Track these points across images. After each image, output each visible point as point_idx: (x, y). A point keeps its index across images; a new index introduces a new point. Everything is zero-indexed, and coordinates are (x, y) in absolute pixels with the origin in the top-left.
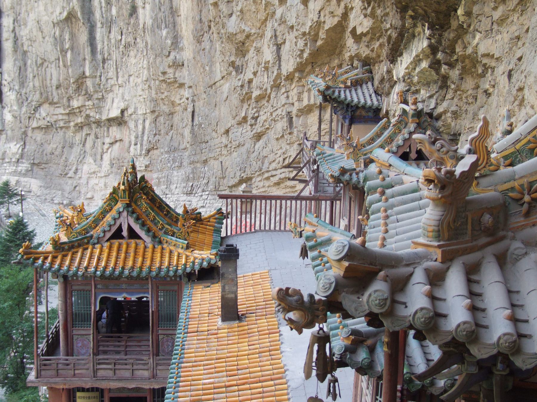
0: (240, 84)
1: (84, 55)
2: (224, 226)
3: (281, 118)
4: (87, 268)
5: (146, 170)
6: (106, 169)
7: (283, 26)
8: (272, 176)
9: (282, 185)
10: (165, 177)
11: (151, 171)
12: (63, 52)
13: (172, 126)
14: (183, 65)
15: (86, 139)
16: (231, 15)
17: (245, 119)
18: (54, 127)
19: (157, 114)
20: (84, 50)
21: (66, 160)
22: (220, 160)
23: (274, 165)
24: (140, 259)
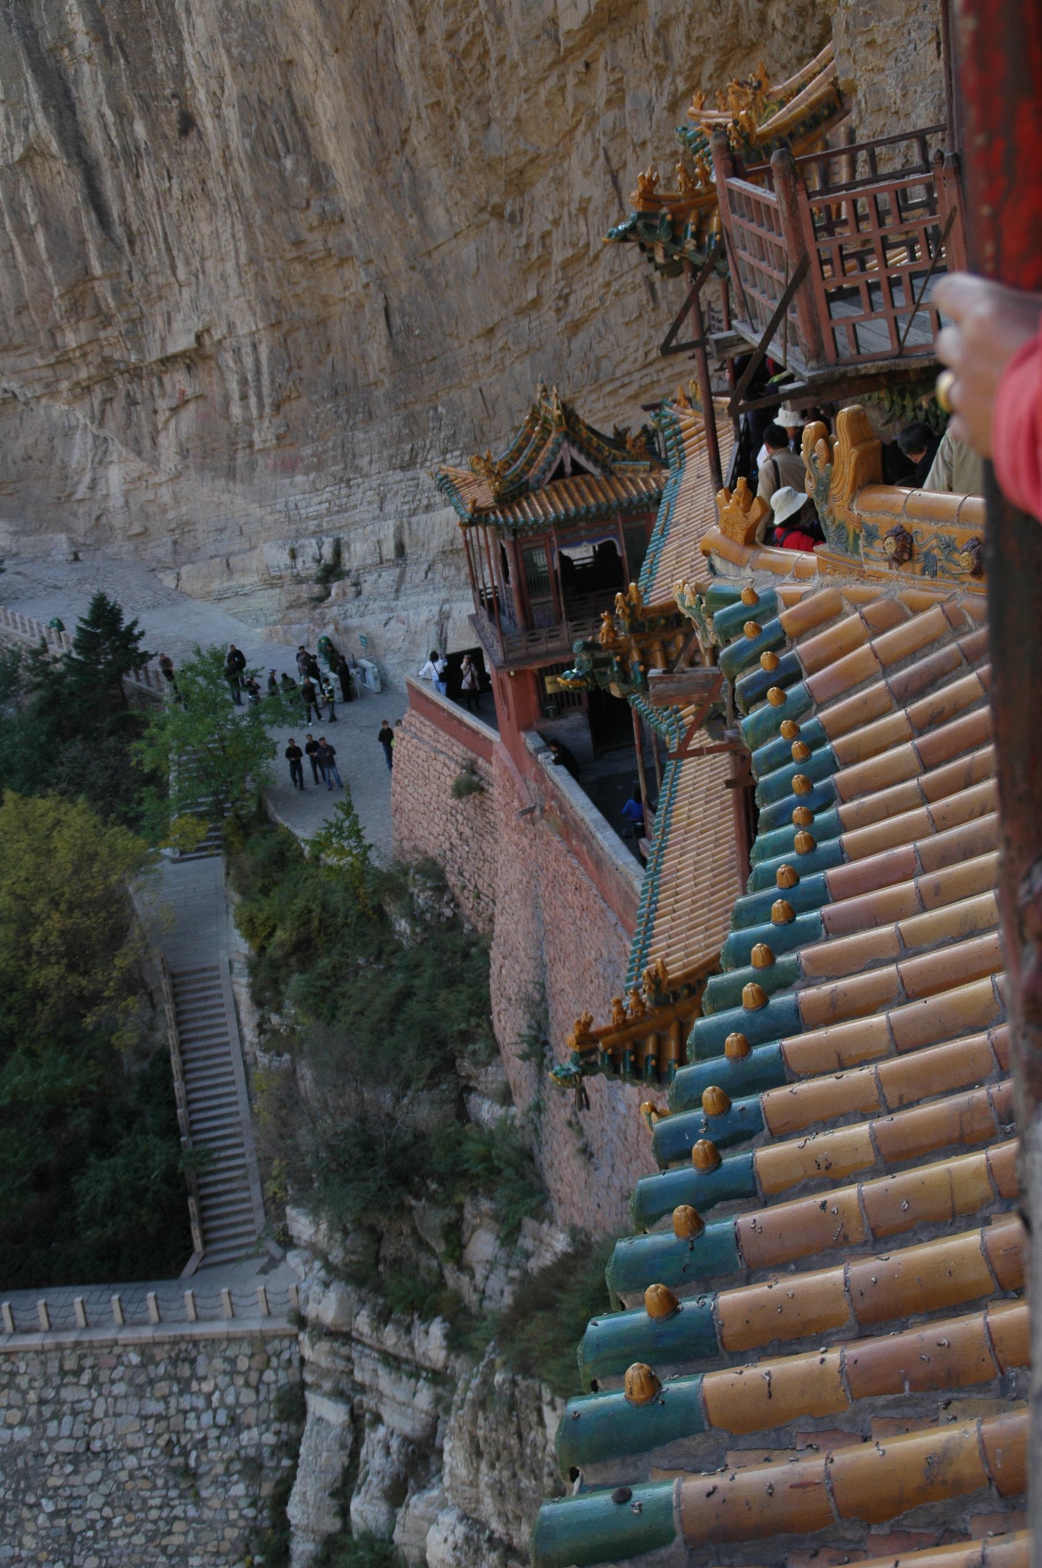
0: (523, 241)
1: (81, 232)
3: (634, 289)
5: (279, 445)
6: (171, 465)
7: (619, 140)
8: (623, 386)
10: (334, 448)
11: (292, 444)
12: (25, 232)
13: (328, 345)
14: (342, 220)
15: (103, 412)
16: (487, 126)
17: (536, 303)
18: (22, 399)
19: (286, 327)
20: (78, 221)
21: (64, 466)
23: (625, 367)
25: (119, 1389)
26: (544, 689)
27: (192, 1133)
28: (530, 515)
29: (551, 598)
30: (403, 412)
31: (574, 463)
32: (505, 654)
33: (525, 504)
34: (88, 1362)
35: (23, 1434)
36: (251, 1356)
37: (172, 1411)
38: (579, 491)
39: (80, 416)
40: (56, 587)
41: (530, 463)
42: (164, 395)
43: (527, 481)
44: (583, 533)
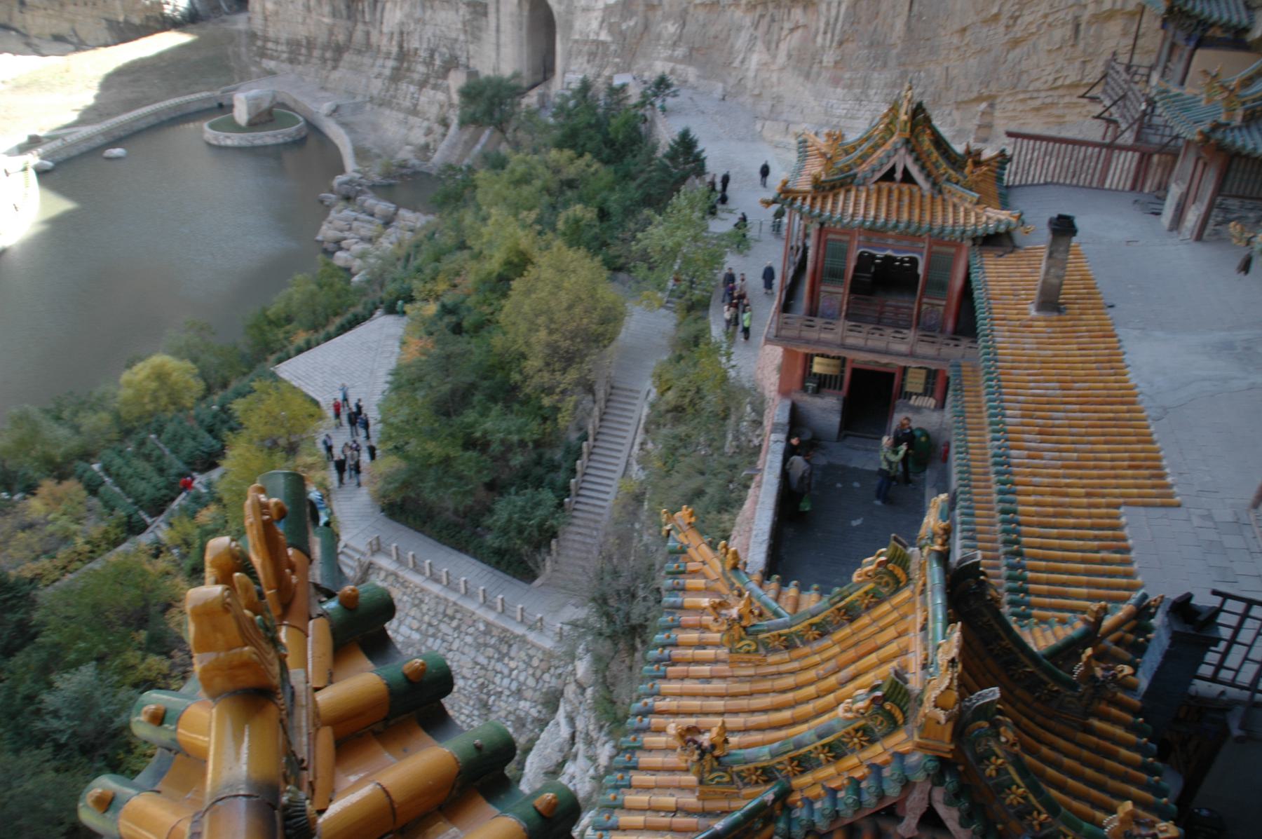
2: (1007, 172)
3: (1063, 24)
4: (853, 215)
8: (1031, 98)
9: (1044, 112)
17: (996, 17)
21: (732, 47)
22: (945, 65)
23: (1037, 84)
24: (917, 212)
25: (469, 639)
26: (811, 367)
27: (578, 495)
28: (839, 210)
29: (841, 290)
30: (902, 68)
31: (906, 172)
32: (779, 329)
33: (841, 197)
34: (459, 616)
35: (416, 636)
36: (542, 660)
37: (490, 668)
38: (900, 200)
39: (748, 21)
40: (703, 113)
41: (863, 158)
42: (789, 19)
43: (855, 175)
44: (890, 241)
